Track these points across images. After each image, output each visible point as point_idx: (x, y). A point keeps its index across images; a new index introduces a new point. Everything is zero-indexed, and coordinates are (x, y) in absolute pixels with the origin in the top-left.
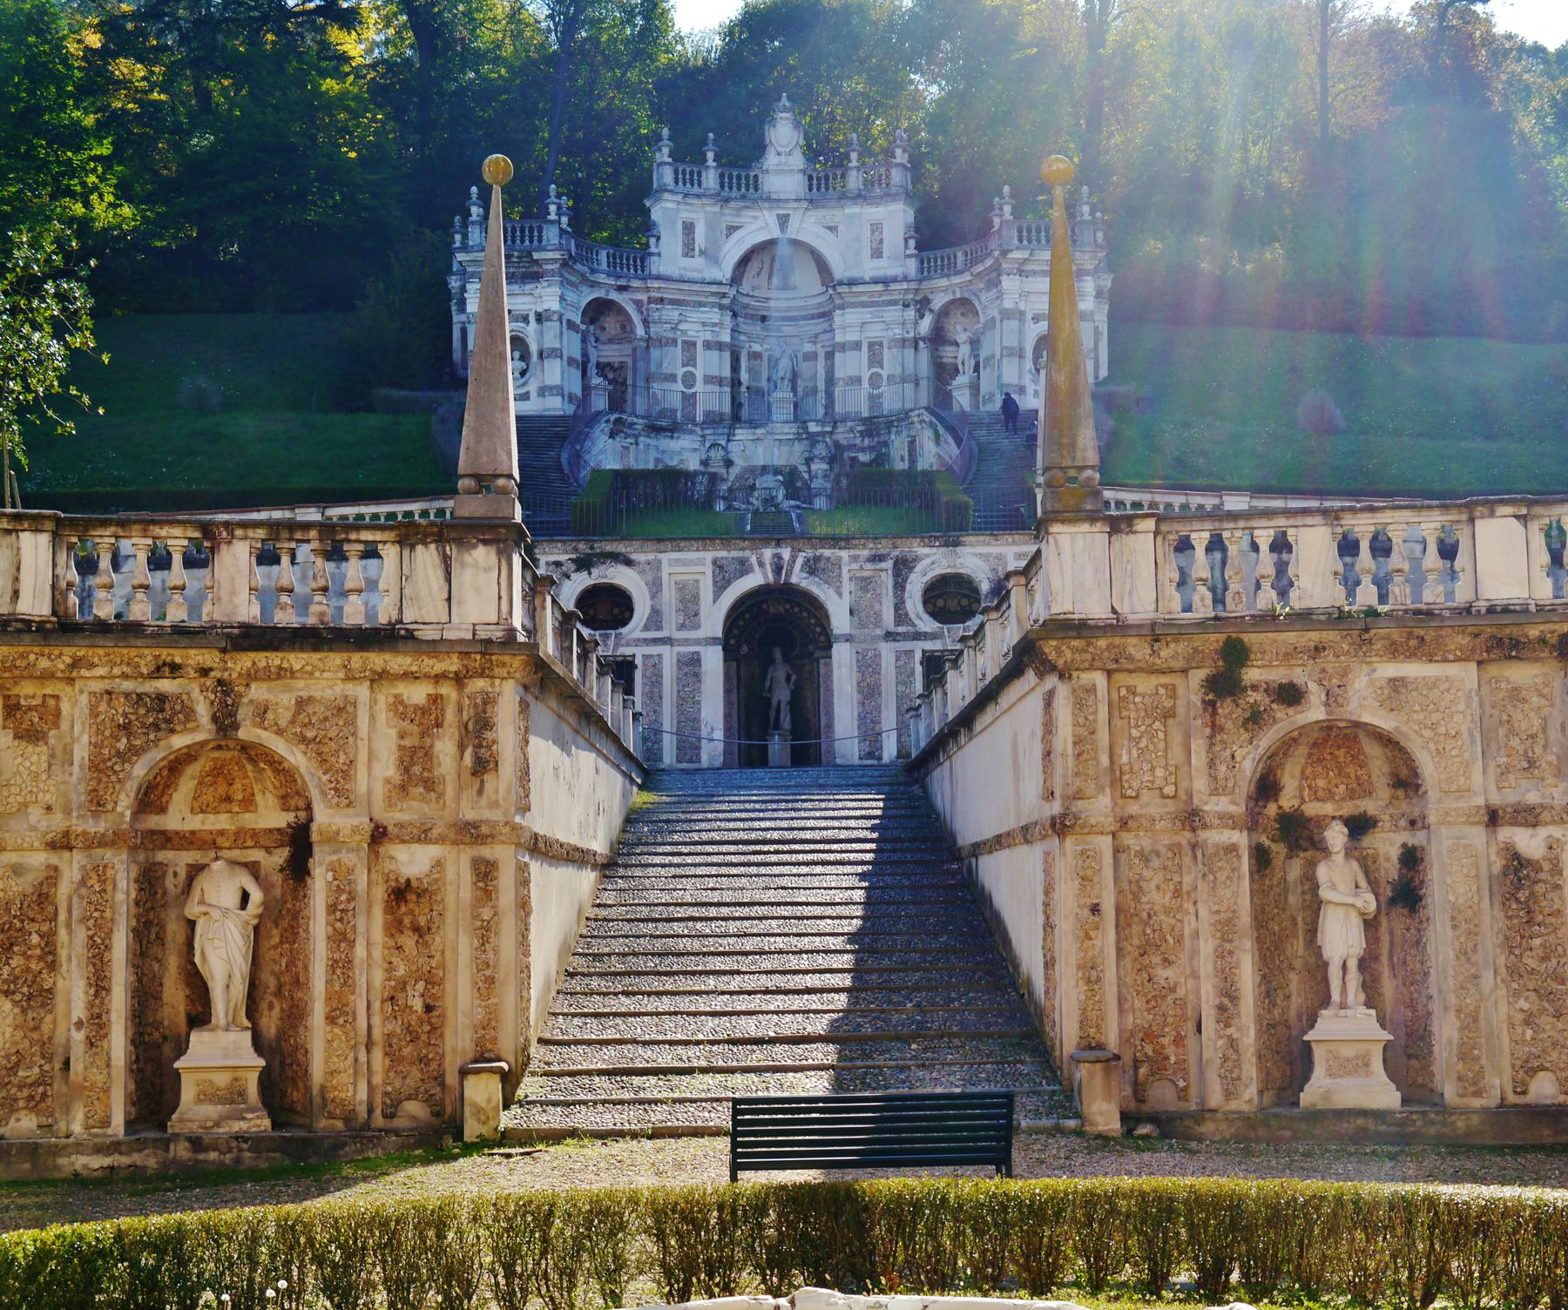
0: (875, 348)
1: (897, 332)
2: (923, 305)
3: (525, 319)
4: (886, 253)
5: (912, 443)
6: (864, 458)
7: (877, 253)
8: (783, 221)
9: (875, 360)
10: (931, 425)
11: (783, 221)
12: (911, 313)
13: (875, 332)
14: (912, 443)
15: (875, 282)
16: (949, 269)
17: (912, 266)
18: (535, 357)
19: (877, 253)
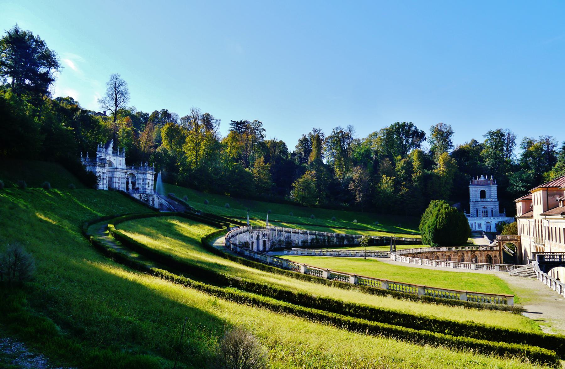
0: (119, 178)
1: (123, 176)
2: (126, 173)
3: (101, 173)
4: (122, 165)
5: (153, 199)
6: (146, 199)
7: (120, 165)
8: (110, 157)
9: (119, 180)
10: (157, 197)
11: (110, 157)
12: (125, 174)
13: (120, 176)
14: (153, 199)
15: (121, 169)
16: (131, 169)
17: (124, 168)
18: (102, 179)
19: (120, 165)
